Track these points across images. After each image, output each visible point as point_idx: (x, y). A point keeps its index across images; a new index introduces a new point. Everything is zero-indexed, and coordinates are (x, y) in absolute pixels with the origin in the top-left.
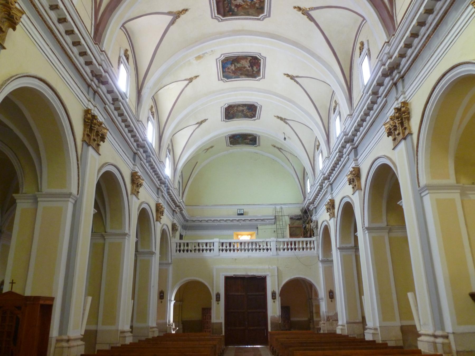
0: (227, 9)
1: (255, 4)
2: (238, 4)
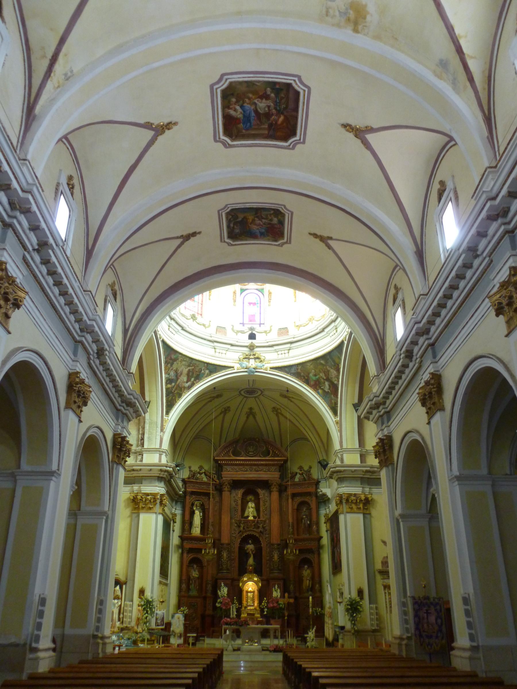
0: (283, 95)
1: (237, 102)
2: (264, 101)
